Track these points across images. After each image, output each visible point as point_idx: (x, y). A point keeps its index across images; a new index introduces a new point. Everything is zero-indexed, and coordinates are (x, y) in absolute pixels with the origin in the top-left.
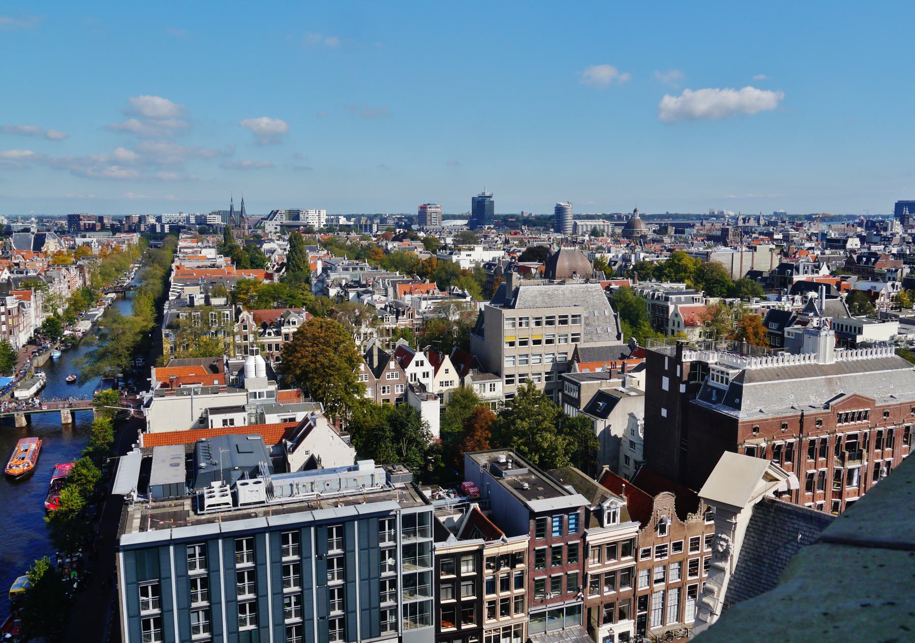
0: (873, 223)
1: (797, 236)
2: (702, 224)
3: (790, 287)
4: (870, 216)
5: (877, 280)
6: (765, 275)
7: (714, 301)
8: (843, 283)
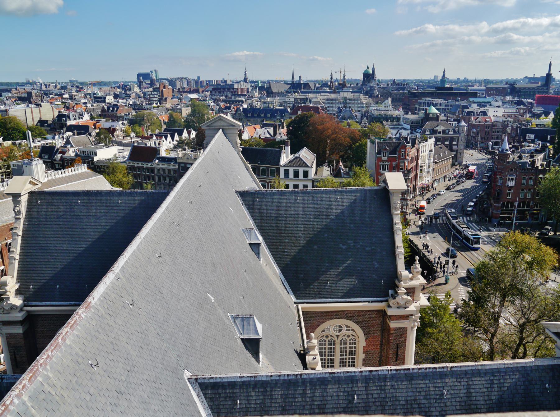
0: (126, 86)
1: (78, 96)
2: (16, 89)
3: (65, 129)
4: (126, 82)
5: (114, 121)
6: (49, 122)
7: (9, 143)
8: (98, 124)
